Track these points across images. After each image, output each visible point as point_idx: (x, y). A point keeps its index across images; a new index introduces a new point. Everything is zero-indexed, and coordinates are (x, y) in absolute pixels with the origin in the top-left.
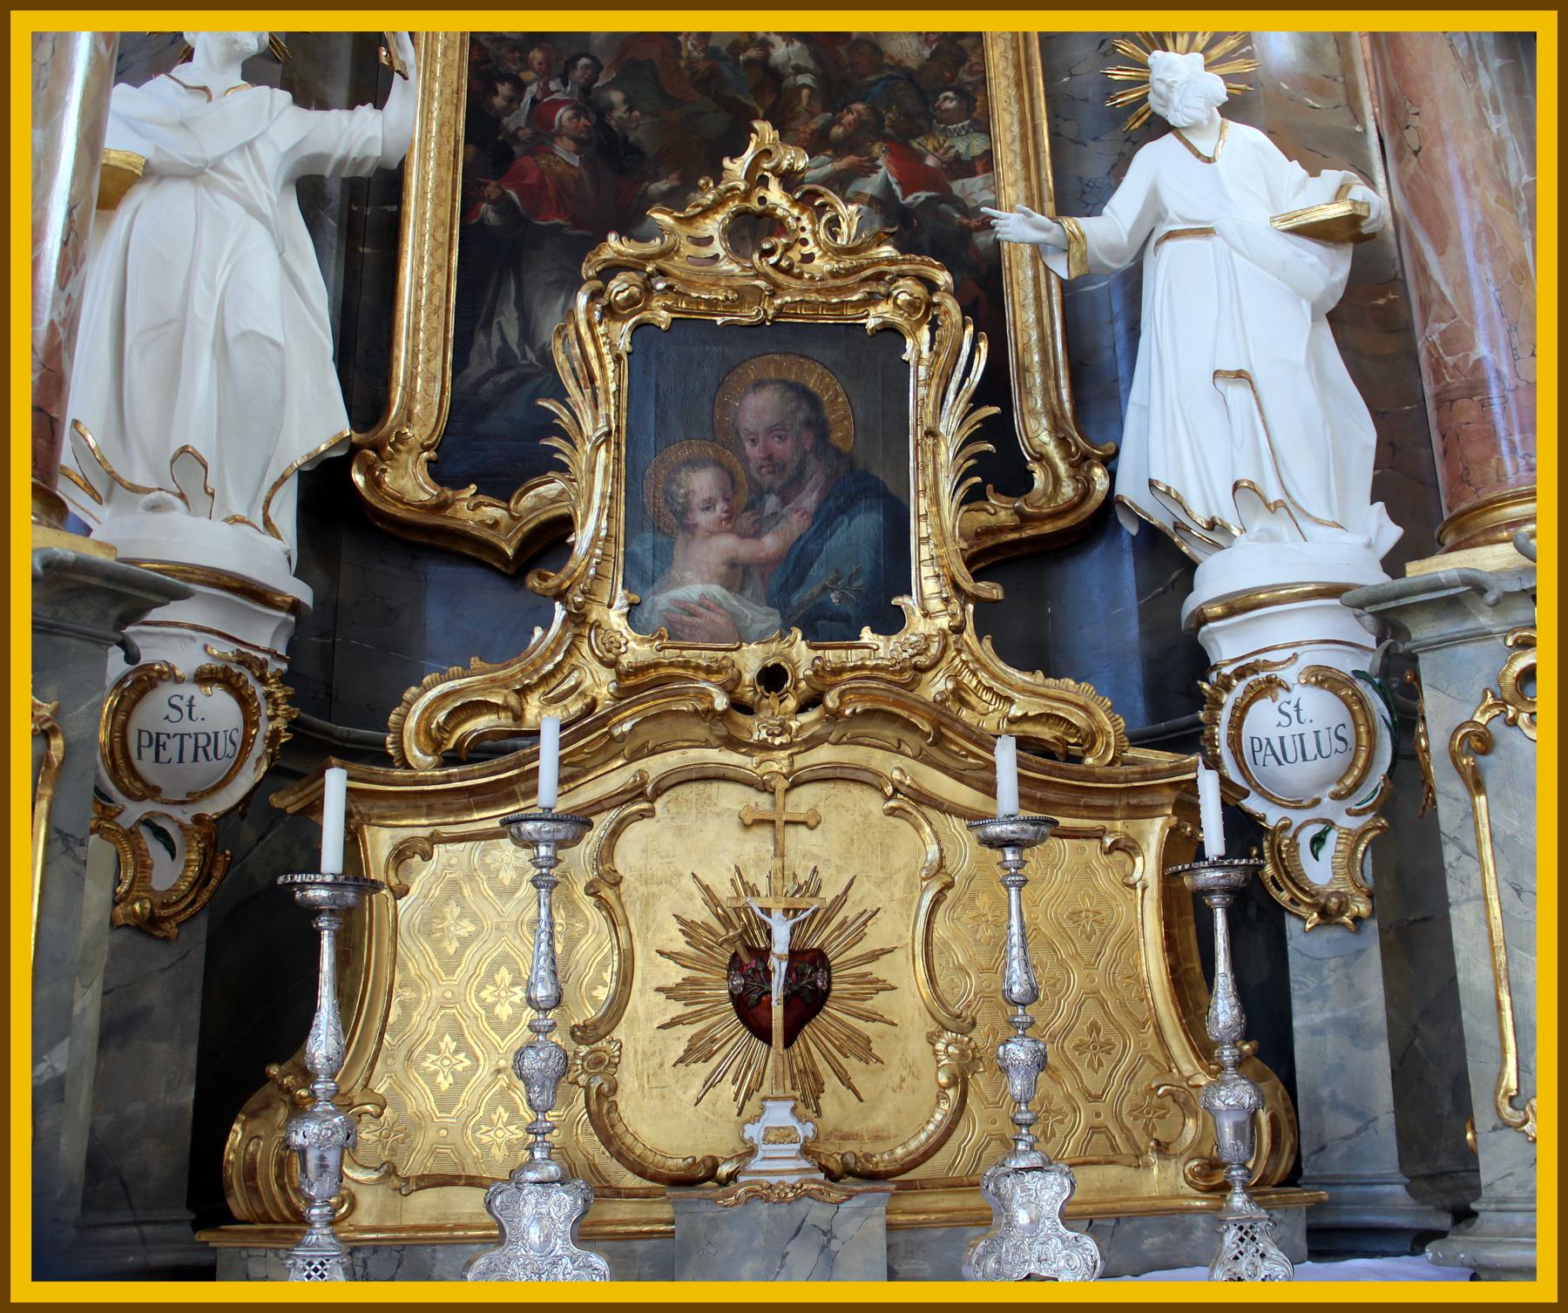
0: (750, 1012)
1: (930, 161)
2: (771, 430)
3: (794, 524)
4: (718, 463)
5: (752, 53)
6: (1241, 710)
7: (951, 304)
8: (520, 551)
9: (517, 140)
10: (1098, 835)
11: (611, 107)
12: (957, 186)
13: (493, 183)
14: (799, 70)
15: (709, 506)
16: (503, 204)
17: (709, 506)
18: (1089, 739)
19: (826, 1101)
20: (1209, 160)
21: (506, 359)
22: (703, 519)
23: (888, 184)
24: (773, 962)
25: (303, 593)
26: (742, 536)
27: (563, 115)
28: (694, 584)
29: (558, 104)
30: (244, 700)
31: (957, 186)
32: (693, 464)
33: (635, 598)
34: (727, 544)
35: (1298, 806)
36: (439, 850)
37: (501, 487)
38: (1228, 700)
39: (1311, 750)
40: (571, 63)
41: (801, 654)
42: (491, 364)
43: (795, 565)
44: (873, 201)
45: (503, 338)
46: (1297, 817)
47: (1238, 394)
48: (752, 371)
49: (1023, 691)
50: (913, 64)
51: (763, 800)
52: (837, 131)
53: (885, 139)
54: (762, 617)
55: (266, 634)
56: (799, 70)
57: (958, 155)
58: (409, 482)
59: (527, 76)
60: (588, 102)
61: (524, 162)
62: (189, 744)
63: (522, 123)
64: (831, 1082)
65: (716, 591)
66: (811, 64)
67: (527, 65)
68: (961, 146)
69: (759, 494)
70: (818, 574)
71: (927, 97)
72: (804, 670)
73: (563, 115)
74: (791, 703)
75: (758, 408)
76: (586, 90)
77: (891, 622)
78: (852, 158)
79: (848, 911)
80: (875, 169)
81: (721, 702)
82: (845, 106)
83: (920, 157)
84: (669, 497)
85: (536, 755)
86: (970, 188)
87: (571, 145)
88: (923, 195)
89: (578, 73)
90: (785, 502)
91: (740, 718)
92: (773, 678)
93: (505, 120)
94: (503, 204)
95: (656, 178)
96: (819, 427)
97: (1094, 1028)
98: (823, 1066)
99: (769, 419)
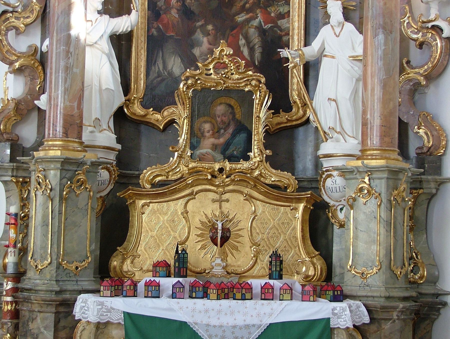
3: (227, 136)
4: (211, 122)
7: (264, 87)
8: (163, 127)
9: (161, 10)
10: (290, 206)
12: (279, 22)
13: (155, 23)
15: (208, 132)
16: (158, 29)
19: (228, 258)
20: (337, 36)
22: (207, 135)
23: (261, 22)
24: (219, 231)
25: (119, 147)
28: (206, 147)
30: (110, 172)
31: (279, 22)
32: (205, 122)
33: (192, 152)
34: (212, 140)
35: (337, 201)
36: (151, 204)
37: (158, 109)
38: (324, 176)
39: (338, 190)
41: (228, 165)
42: (156, 75)
43: (227, 145)
44: (256, 27)
45: (159, 68)
46: (337, 204)
47: (333, 103)
48: (219, 101)
49: (275, 175)
52: (247, 6)
53: (260, 8)
54: (219, 156)
55: (112, 157)
57: (280, 12)
58: (138, 109)
61: (163, 16)
62: (100, 182)
63: (163, 4)
64: (230, 255)
65: (209, 150)
68: (281, 10)
69: (219, 129)
74: (225, 176)
75: (220, 109)
77: (247, 158)
78: (251, 14)
79: (235, 220)
80: (257, 17)
81: (209, 177)
83: (269, 13)
84: (200, 130)
87: (176, 11)
88: (270, 25)
90: (225, 131)
91: (214, 179)
92: (221, 170)
93: (158, 3)
94: (158, 29)
95: (198, 21)
96: (233, 114)
97: (285, 247)
98: (228, 251)
99: (222, 112)
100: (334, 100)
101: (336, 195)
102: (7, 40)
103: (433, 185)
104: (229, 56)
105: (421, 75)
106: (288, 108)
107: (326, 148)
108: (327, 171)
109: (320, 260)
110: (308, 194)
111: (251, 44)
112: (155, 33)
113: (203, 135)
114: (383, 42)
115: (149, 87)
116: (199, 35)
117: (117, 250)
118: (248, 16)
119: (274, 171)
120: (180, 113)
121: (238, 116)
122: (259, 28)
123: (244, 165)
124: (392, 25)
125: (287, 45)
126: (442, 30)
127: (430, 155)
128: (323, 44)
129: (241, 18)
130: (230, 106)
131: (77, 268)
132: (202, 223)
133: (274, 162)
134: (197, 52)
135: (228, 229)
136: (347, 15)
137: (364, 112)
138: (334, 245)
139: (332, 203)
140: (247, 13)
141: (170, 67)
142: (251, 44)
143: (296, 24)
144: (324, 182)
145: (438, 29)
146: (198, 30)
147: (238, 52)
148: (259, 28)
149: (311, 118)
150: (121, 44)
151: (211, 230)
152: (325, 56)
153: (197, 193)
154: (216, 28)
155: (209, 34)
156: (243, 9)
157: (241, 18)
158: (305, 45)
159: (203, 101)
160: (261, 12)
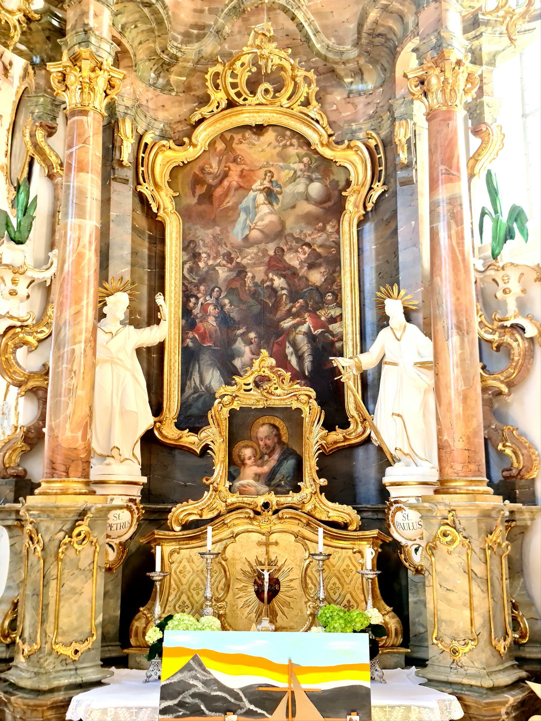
1: (323, 319)
2: (266, 437)
4: (252, 447)
5: (268, 283)
6: (395, 513)
7: (315, 403)
8: (200, 452)
9: (197, 318)
10: (353, 549)
11: (225, 305)
12: (331, 327)
13: (190, 332)
14: (282, 289)
15: (250, 458)
16: (193, 339)
17: (250, 458)
18: (351, 523)
19: (278, 618)
20: (399, 340)
22: (248, 462)
23: (309, 327)
24: (265, 584)
25: (144, 480)
26: (258, 466)
27: (211, 308)
29: (209, 304)
30: (132, 512)
31: (331, 327)
32: (246, 447)
33: (231, 484)
35: (411, 540)
36: (182, 551)
37: (195, 430)
38: (392, 509)
39: (411, 528)
40: (213, 290)
41: (273, 499)
42: (191, 391)
43: (273, 473)
44: (305, 334)
45: (195, 383)
46: (410, 543)
47: (399, 419)
48: (261, 421)
49: (332, 509)
50: (318, 284)
51: (264, 537)
52: (294, 310)
53: (309, 311)
54: (264, 489)
55: (136, 492)
56: (282, 289)
57: (332, 316)
58: (169, 432)
59: (199, 295)
60: (219, 305)
61: (199, 325)
62: (119, 526)
63: (198, 312)
64: (280, 613)
65: (252, 482)
66: (286, 286)
70: (278, 477)
71: (322, 296)
72: (274, 503)
73: (211, 308)
74: (271, 513)
75: (263, 431)
77: (297, 489)
78: (298, 319)
79: (285, 568)
80: (305, 322)
81: (252, 515)
83: (319, 317)
84: (239, 456)
87: (213, 319)
88: (320, 330)
89: (215, 294)
90: (270, 457)
91: (257, 517)
92: (266, 505)
93: (193, 311)
94: (193, 339)
95: (239, 329)
98: (277, 609)
99: (266, 434)
100: (399, 415)
101: (409, 533)
102: (15, 358)
103: (527, 516)
104: (271, 368)
105: (502, 382)
106: (345, 425)
108: (396, 502)
109: (393, 618)
110: (374, 533)
111: (300, 353)
112: (191, 344)
113: (244, 464)
114: (458, 344)
115: (184, 406)
116: (239, 344)
117: (139, 611)
118: (295, 321)
119: (330, 504)
120: (214, 436)
121: (284, 439)
123: (293, 498)
124: (468, 324)
125: (341, 354)
126: (523, 329)
127: (521, 479)
128: (383, 348)
129: (287, 324)
130: (274, 426)
131: (76, 652)
132: (244, 572)
133: (332, 493)
134: (237, 363)
135: (277, 580)
136: (408, 315)
137: (440, 433)
138: (410, 595)
139: (403, 542)
140: (294, 318)
141: (207, 382)
142: (300, 353)
143: (349, 329)
144: (393, 517)
145: (519, 328)
146: (239, 339)
147: (282, 362)
149: (373, 435)
151: (255, 583)
152: (386, 363)
153: (237, 535)
154: (260, 337)
155: (252, 343)
156: (289, 314)
157: (287, 324)
158: (362, 352)
160: (310, 316)
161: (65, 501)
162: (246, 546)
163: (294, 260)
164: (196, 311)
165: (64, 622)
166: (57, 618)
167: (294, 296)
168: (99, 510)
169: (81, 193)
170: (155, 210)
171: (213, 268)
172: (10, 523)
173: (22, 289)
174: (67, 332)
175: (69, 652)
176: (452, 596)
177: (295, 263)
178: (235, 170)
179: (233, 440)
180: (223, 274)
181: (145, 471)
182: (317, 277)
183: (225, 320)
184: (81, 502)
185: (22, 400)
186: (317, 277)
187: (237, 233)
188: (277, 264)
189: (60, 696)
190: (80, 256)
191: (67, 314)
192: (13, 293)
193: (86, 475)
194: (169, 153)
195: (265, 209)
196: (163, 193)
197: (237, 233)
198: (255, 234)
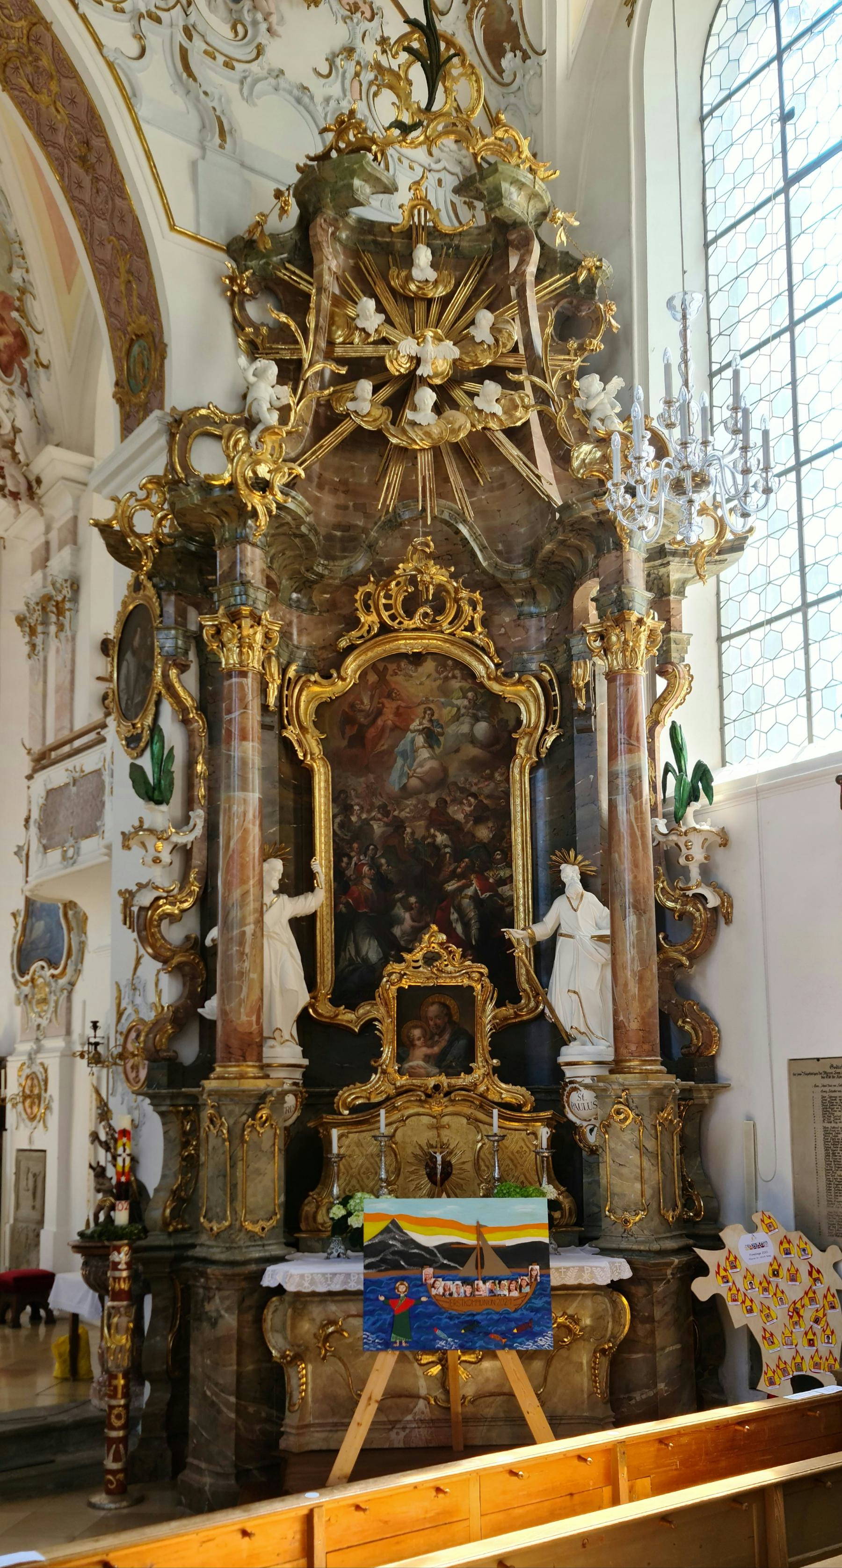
0: (431, 1176)
1: (491, 880)
2: (436, 1017)
3: (443, 1043)
5: (429, 840)
6: (569, 1093)
7: (487, 980)
11: (381, 865)
12: (500, 889)
14: (446, 846)
15: (419, 1039)
16: (347, 904)
17: (419, 1039)
18: (525, 1104)
21: (351, 961)
22: (418, 1043)
25: (306, 1062)
26: (428, 1047)
27: (366, 869)
29: (364, 864)
31: (500, 889)
32: (415, 1027)
34: (425, 1050)
38: (568, 1089)
40: (367, 848)
41: (444, 1080)
42: (347, 963)
43: (444, 1053)
44: (471, 897)
46: (585, 1124)
47: (574, 996)
48: (430, 1000)
50: (486, 841)
51: (435, 1120)
52: (459, 870)
55: (298, 1075)
56: (446, 846)
58: (325, 1009)
59: (353, 854)
60: (374, 865)
61: (354, 888)
65: (421, 1063)
66: (450, 843)
67: (352, 850)
68: (502, 874)
70: (450, 1057)
71: (491, 855)
72: (445, 1085)
73: (366, 869)
75: (433, 1010)
76: (373, 858)
80: (472, 885)
81: (423, 1098)
82: (462, 860)
83: (487, 879)
84: (409, 1037)
85: (379, 1121)
86: (504, 890)
88: (488, 894)
89: (370, 852)
92: (437, 1087)
94: (347, 904)
96: (449, 1015)
100: (575, 992)
101: (584, 1113)
102: (160, 932)
103: (705, 1094)
104: (441, 944)
105: (683, 954)
106: (516, 1000)
107: (568, 1053)
108: (571, 1082)
109: (567, 1197)
110: (547, 1114)
111: (466, 919)
112: (344, 910)
113: (413, 1045)
115: (339, 979)
117: (308, 1196)
118: (460, 884)
119: (503, 1085)
121: (455, 1018)
122: (475, 898)
123: (464, 1080)
125: (512, 926)
127: (700, 1056)
128: (558, 918)
129: (451, 886)
130: (444, 1005)
131: (263, 1229)
132: (415, 1156)
133: (505, 1074)
134: (397, 931)
135: (449, 1162)
139: (578, 1122)
140: (459, 881)
141: (364, 953)
142: (466, 919)
143: (521, 891)
144: (568, 1097)
146: (399, 904)
147: (452, 937)
148: (475, 898)
149: (547, 1011)
150: (303, 928)
151: (427, 1166)
152: (561, 935)
153: (408, 1118)
154: (420, 901)
155: (412, 909)
156: (453, 875)
157: (451, 886)
158: (534, 922)
159: (410, 1002)
160: (477, 878)
161: (248, 1085)
162: (416, 1130)
163: (458, 813)
164: (349, 872)
165: (251, 1200)
166: (244, 1197)
167: (458, 856)
168: (279, 1094)
169: (244, 763)
170: (301, 755)
171: (366, 822)
172: (164, 1109)
173: (166, 857)
174: (235, 914)
175: (257, 1229)
176: (624, 1171)
177: (460, 817)
178: (390, 707)
179: (402, 1020)
180: (378, 828)
181: (305, 1055)
182: (484, 833)
183: (380, 880)
184: (262, 1084)
185: (165, 978)
186: (484, 833)
187: (394, 782)
188: (439, 818)
189: (253, 1267)
190: (246, 832)
191: (236, 894)
192: (157, 860)
193: (260, 1058)
194: (316, 689)
195: (424, 754)
196: (309, 736)
197: (394, 782)
198: (414, 782)
